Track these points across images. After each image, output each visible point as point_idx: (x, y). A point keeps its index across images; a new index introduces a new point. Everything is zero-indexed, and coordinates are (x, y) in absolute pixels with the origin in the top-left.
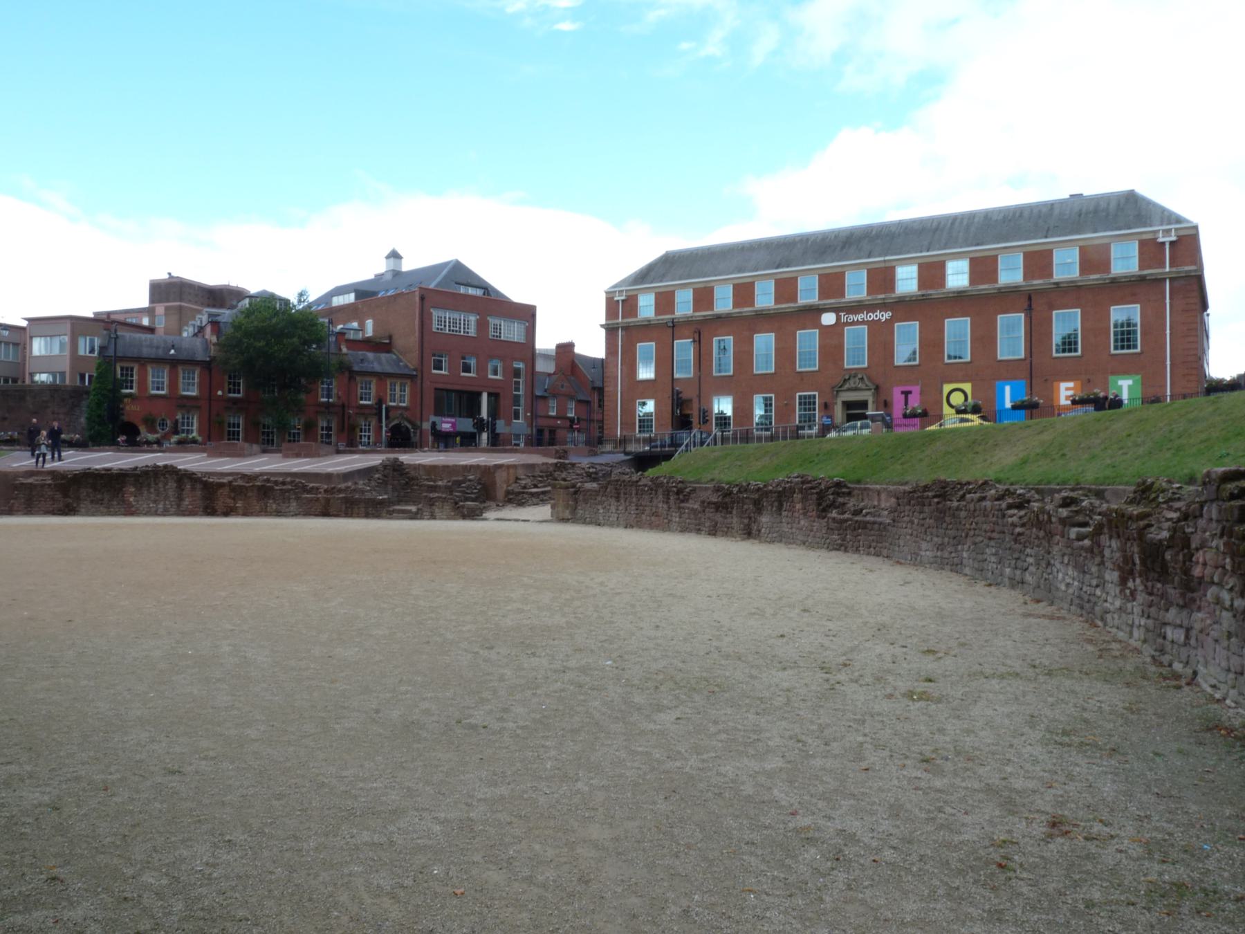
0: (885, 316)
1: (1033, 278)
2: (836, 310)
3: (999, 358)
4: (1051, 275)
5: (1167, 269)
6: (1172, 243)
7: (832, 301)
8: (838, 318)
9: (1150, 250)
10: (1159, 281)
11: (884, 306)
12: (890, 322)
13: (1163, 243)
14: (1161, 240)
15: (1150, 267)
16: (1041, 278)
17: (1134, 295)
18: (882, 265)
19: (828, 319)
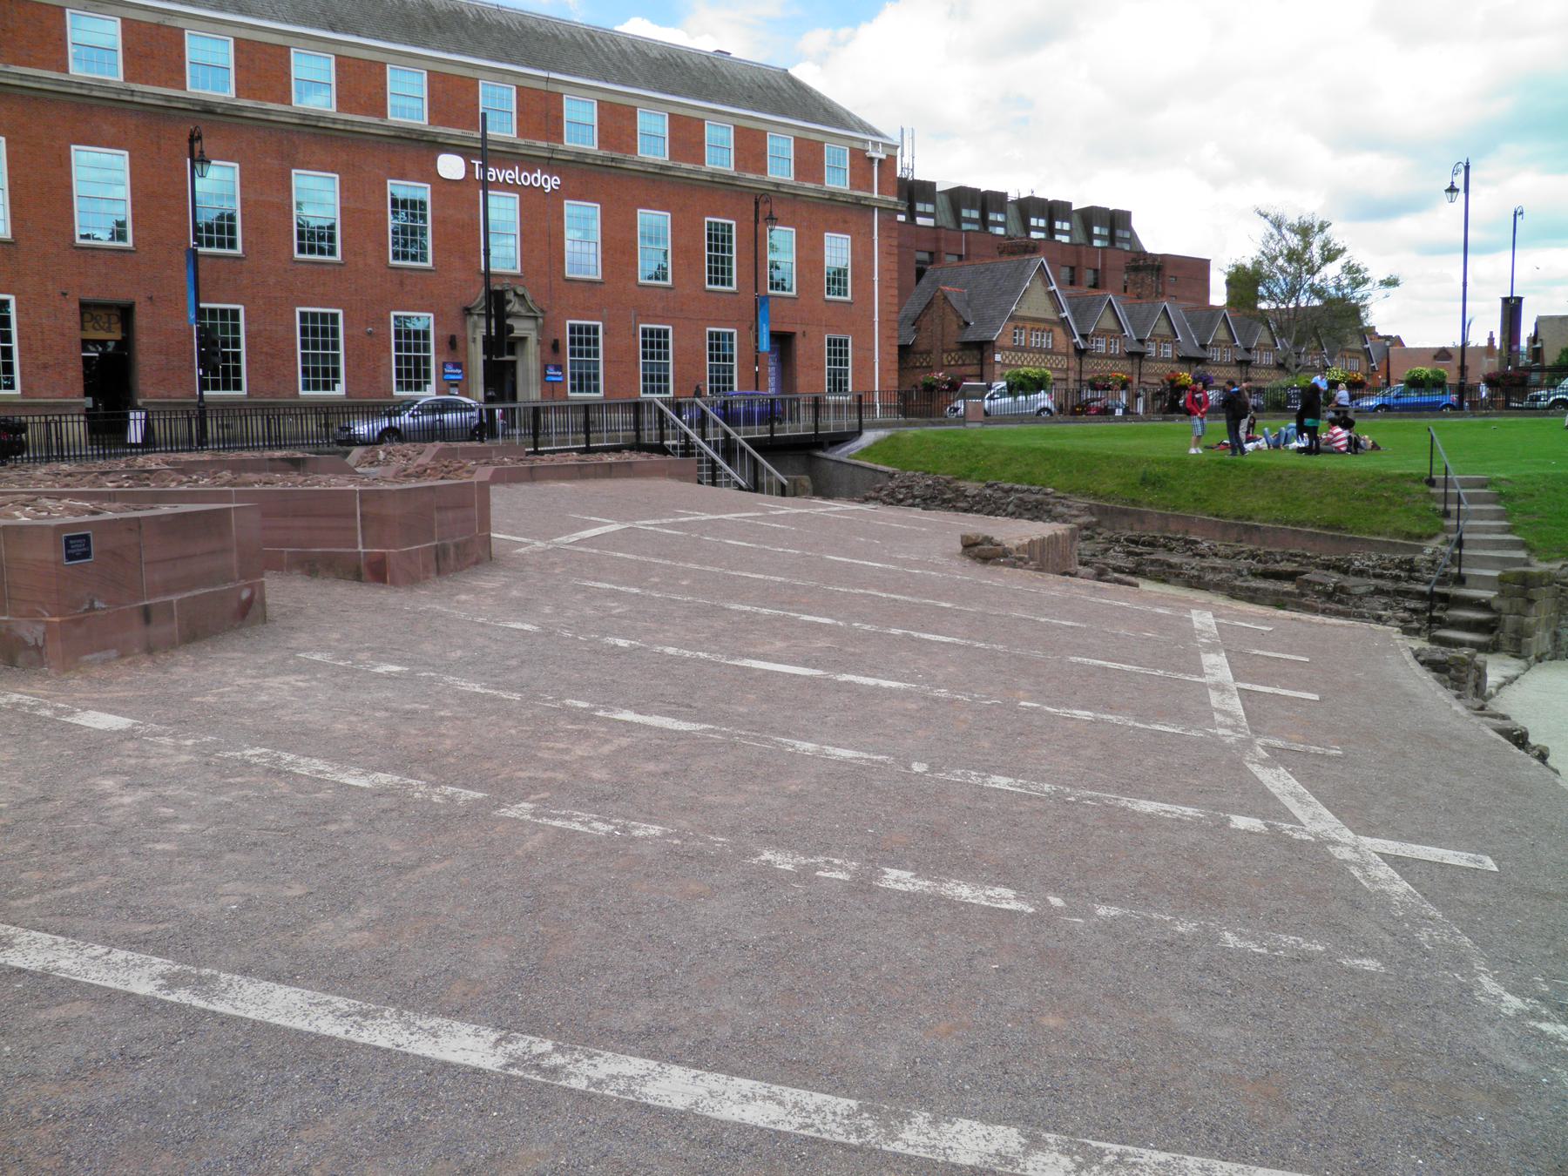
0: (553, 182)
1: (746, 169)
2: (464, 152)
3: (568, 275)
4: (764, 171)
5: (876, 195)
6: (880, 161)
7: (457, 132)
8: (470, 169)
9: (861, 161)
10: (861, 207)
11: (550, 164)
12: (557, 196)
13: (872, 159)
14: (874, 155)
15: (859, 189)
16: (755, 171)
17: (845, 222)
18: (542, 86)
19: (451, 166)
